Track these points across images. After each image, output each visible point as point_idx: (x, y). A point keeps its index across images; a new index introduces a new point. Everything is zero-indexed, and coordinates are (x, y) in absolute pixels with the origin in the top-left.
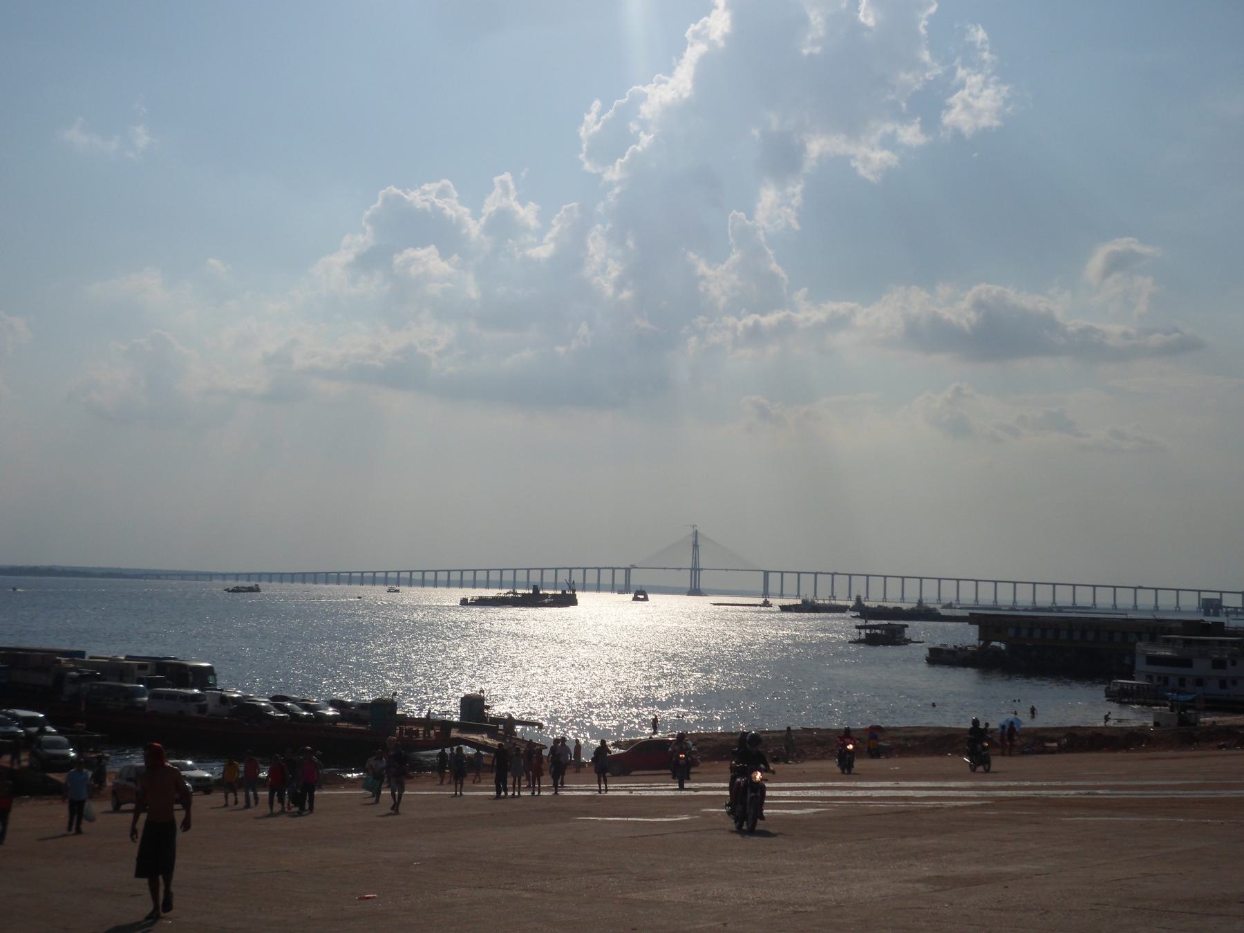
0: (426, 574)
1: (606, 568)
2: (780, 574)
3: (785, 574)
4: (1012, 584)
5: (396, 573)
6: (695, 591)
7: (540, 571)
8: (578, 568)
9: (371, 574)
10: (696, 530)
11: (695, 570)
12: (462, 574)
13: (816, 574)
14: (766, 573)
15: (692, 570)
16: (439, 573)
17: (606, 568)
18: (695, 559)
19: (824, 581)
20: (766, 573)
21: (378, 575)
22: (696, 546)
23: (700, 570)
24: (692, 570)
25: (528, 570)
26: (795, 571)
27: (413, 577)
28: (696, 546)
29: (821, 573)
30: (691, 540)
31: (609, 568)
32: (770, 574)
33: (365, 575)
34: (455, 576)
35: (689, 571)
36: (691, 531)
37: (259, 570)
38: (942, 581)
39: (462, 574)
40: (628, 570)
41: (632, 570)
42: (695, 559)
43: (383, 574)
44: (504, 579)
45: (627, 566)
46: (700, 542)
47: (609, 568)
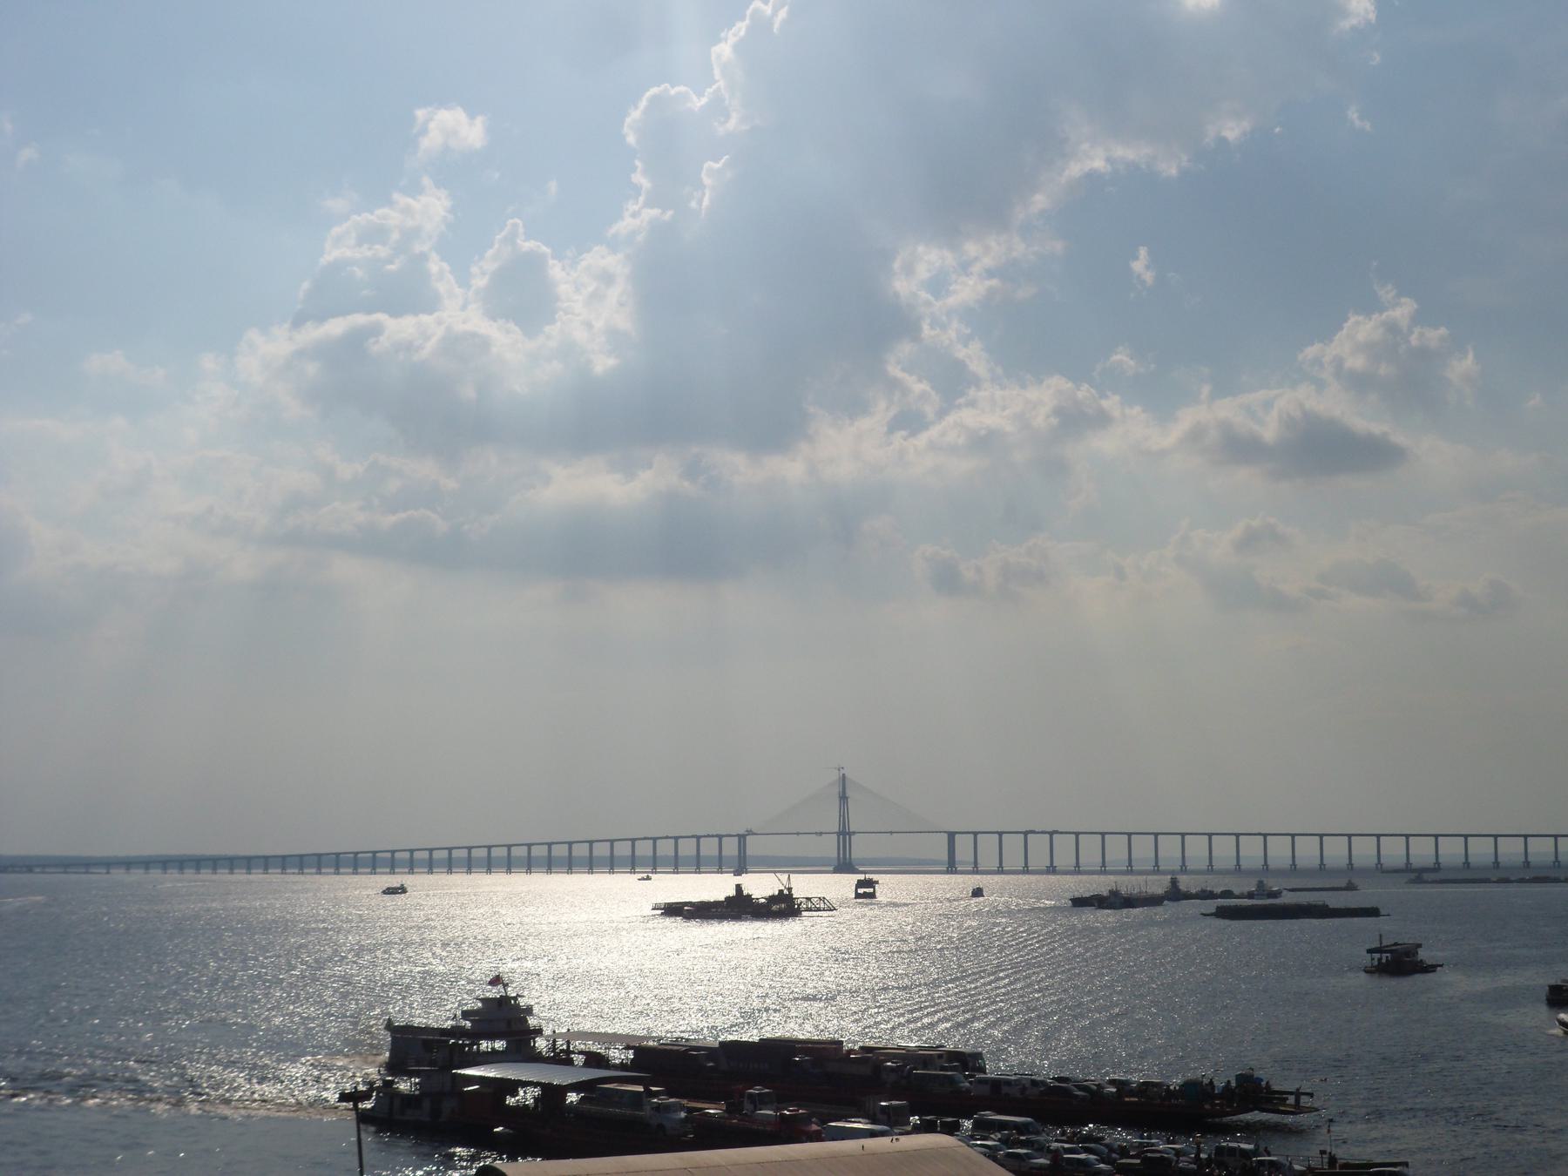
0: (575, 846)
1: (708, 836)
4: (1346, 838)
5: (466, 851)
6: (951, 868)
7: (716, 839)
8: (667, 837)
11: (844, 834)
12: (633, 846)
14: (951, 836)
15: (839, 834)
17: (708, 836)
20: (951, 836)
21: (475, 853)
22: (843, 798)
23: (851, 834)
24: (839, 834)
26: (1097, 831)
27: (554, 853)
28: (843, 798)
30: (836, 790)
31: (713, 836)
34: (687, 848)
35: (835, 836)
36: (835, 776)
37: (230, 852)
38: (1382, 838)
39: (633, 846)
40: (742, 838)
41: (748, 837)
46: (849, 793)
47: (713, 836)
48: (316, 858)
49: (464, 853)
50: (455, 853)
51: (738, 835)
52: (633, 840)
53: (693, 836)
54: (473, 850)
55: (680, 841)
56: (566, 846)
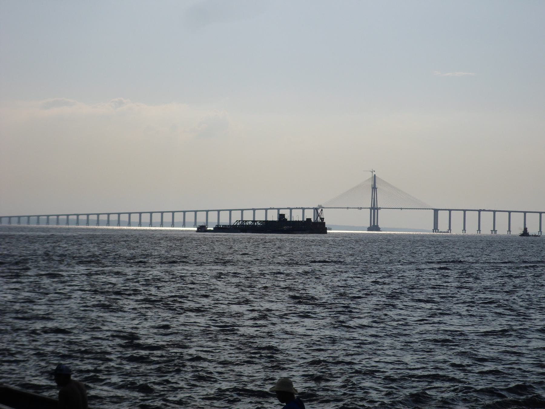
1: (297, 208)
2: (523, 214)
3: (512, 213)
8: (273, 209)
9: (56, 217)
10: (375, 175)
11: (374, 209)
13: (480, 211)
14: (436, 211)
15: (371, 209)
16: (132, 215)
17: (297, 208)
18: (374, 200)
19: (487, 217)
20: (436, 211)
22: (374, 188)
23: (378, 209)
24: (371, 209)
25: (196, 212)
28: (374, 188)
29: (484, 210)
31: (299, 208)
32: (439, 212)
33: (70, 217)
35: (369, 210)
36: (370, 175)
42: (374, 200)
43: (75, 217)
44: (132, 220)
45: (316, 207)
46: (377, 185)
47: (299, 208)
48: (17, 218)
49: (85, 217)
50: (81, 217)
51: (313, 208)
52: (242, 210)
53: (288, 208)
54: (100, 216)
55: (232, 212)
56: (127, 215)
